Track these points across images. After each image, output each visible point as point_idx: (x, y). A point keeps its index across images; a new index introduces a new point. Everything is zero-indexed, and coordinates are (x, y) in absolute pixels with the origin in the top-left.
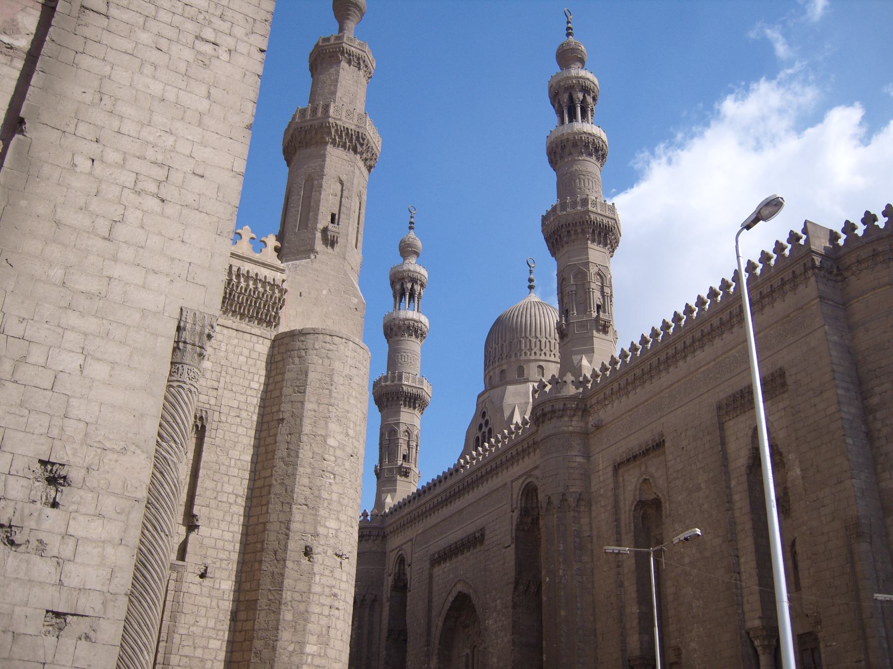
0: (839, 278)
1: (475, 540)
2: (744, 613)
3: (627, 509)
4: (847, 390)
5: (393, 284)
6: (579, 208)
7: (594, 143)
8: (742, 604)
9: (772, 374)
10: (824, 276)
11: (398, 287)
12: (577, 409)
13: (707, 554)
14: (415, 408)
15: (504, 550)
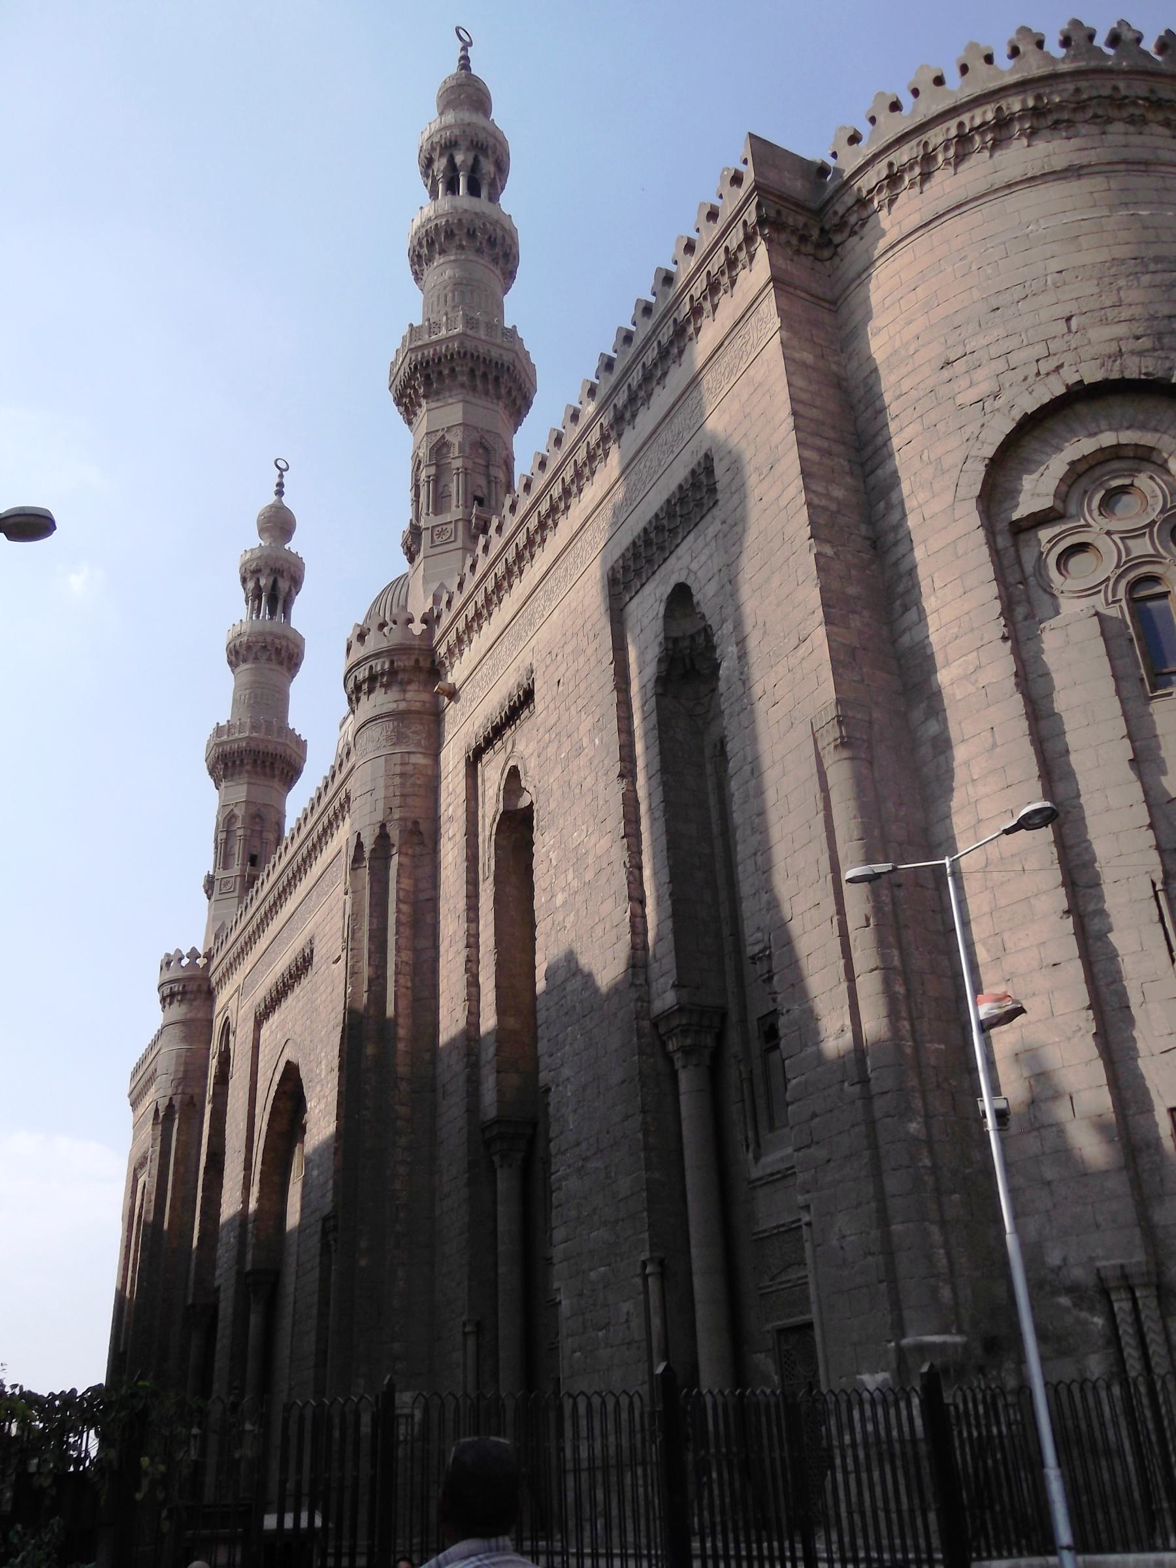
0: (826, 253)
1: (303, 965)
2: (647, 982)
3: (487, 833)
4: (825, 452)
5: (244, 581)
6: (444, 331)
7: (484, 230)
8: (646, 966)
9: (693, 472)
10: (788, 243)
11: (251, 585)
12: (417, 668)
13: (589, 876)
14: (273, 776)
15: (334, 966)
